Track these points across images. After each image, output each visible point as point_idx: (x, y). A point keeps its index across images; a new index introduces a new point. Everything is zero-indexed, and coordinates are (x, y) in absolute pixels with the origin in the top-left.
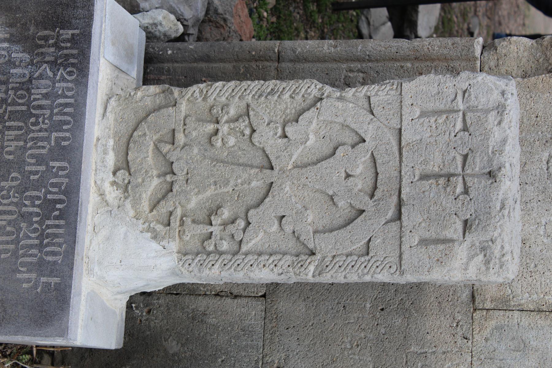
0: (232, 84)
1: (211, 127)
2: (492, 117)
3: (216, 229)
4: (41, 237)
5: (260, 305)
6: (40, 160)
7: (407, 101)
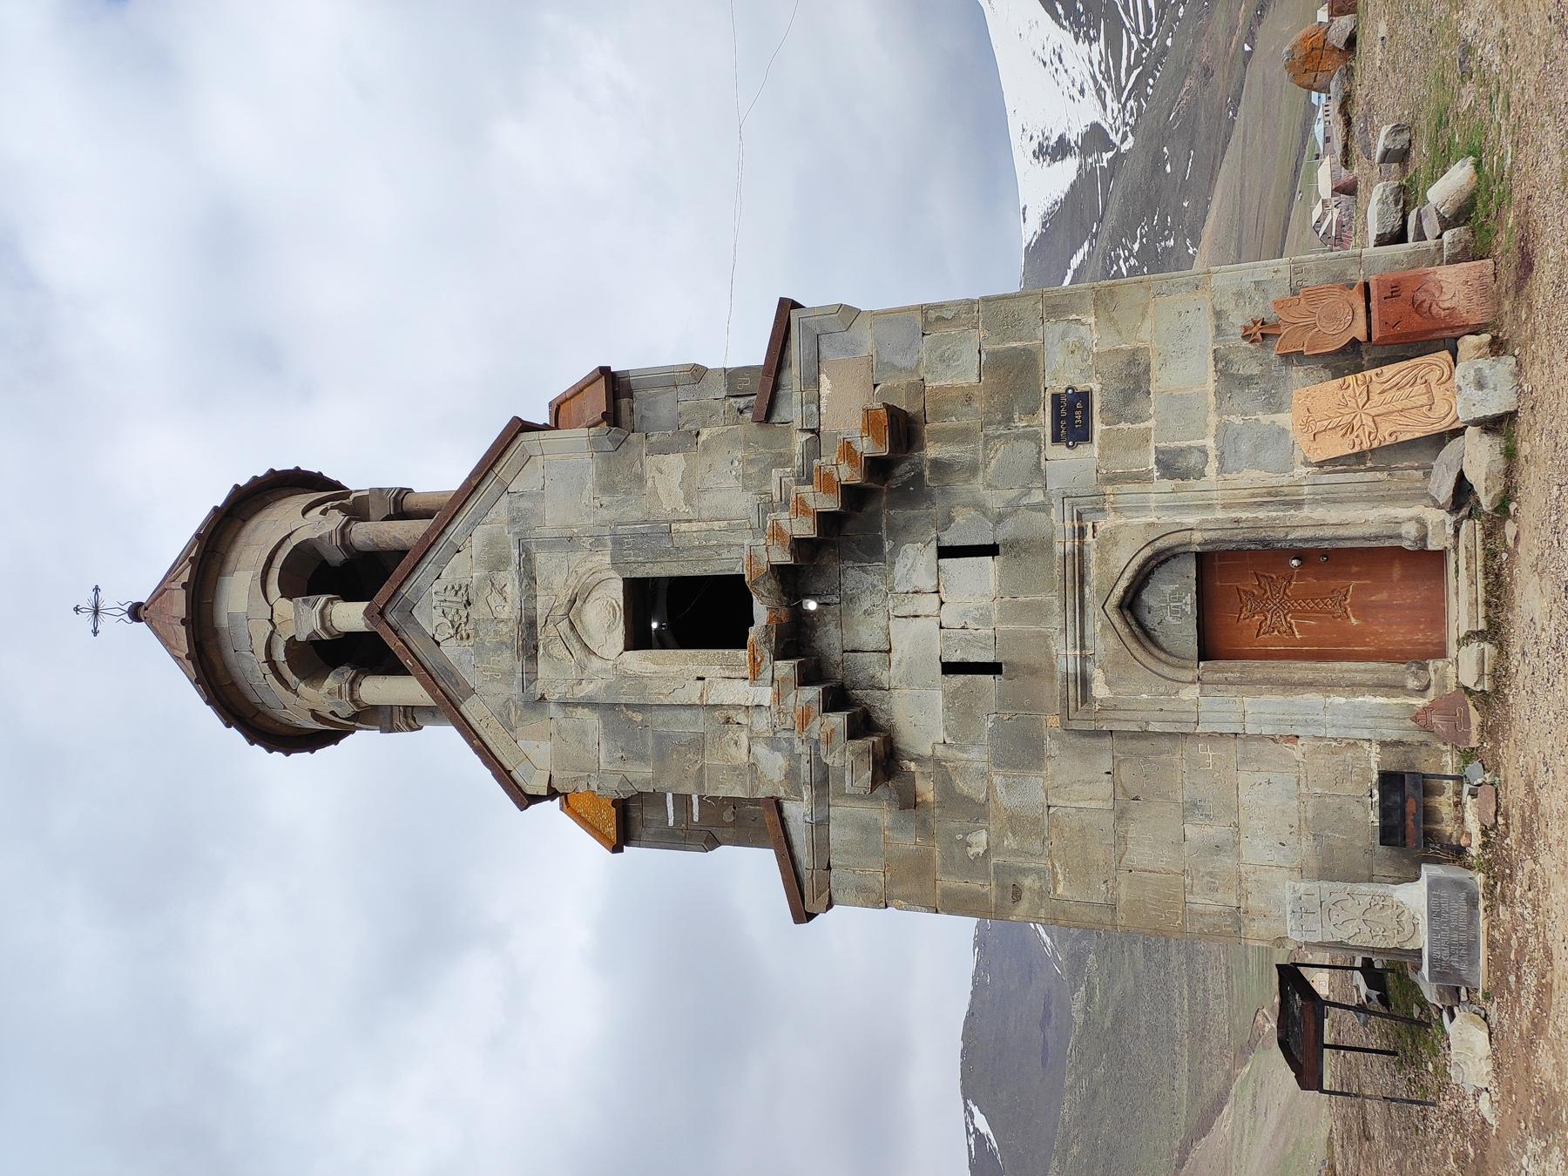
0: (1379, 946)
1: (1385, 934)
3: (1381, 903)
6: (1444, 930)
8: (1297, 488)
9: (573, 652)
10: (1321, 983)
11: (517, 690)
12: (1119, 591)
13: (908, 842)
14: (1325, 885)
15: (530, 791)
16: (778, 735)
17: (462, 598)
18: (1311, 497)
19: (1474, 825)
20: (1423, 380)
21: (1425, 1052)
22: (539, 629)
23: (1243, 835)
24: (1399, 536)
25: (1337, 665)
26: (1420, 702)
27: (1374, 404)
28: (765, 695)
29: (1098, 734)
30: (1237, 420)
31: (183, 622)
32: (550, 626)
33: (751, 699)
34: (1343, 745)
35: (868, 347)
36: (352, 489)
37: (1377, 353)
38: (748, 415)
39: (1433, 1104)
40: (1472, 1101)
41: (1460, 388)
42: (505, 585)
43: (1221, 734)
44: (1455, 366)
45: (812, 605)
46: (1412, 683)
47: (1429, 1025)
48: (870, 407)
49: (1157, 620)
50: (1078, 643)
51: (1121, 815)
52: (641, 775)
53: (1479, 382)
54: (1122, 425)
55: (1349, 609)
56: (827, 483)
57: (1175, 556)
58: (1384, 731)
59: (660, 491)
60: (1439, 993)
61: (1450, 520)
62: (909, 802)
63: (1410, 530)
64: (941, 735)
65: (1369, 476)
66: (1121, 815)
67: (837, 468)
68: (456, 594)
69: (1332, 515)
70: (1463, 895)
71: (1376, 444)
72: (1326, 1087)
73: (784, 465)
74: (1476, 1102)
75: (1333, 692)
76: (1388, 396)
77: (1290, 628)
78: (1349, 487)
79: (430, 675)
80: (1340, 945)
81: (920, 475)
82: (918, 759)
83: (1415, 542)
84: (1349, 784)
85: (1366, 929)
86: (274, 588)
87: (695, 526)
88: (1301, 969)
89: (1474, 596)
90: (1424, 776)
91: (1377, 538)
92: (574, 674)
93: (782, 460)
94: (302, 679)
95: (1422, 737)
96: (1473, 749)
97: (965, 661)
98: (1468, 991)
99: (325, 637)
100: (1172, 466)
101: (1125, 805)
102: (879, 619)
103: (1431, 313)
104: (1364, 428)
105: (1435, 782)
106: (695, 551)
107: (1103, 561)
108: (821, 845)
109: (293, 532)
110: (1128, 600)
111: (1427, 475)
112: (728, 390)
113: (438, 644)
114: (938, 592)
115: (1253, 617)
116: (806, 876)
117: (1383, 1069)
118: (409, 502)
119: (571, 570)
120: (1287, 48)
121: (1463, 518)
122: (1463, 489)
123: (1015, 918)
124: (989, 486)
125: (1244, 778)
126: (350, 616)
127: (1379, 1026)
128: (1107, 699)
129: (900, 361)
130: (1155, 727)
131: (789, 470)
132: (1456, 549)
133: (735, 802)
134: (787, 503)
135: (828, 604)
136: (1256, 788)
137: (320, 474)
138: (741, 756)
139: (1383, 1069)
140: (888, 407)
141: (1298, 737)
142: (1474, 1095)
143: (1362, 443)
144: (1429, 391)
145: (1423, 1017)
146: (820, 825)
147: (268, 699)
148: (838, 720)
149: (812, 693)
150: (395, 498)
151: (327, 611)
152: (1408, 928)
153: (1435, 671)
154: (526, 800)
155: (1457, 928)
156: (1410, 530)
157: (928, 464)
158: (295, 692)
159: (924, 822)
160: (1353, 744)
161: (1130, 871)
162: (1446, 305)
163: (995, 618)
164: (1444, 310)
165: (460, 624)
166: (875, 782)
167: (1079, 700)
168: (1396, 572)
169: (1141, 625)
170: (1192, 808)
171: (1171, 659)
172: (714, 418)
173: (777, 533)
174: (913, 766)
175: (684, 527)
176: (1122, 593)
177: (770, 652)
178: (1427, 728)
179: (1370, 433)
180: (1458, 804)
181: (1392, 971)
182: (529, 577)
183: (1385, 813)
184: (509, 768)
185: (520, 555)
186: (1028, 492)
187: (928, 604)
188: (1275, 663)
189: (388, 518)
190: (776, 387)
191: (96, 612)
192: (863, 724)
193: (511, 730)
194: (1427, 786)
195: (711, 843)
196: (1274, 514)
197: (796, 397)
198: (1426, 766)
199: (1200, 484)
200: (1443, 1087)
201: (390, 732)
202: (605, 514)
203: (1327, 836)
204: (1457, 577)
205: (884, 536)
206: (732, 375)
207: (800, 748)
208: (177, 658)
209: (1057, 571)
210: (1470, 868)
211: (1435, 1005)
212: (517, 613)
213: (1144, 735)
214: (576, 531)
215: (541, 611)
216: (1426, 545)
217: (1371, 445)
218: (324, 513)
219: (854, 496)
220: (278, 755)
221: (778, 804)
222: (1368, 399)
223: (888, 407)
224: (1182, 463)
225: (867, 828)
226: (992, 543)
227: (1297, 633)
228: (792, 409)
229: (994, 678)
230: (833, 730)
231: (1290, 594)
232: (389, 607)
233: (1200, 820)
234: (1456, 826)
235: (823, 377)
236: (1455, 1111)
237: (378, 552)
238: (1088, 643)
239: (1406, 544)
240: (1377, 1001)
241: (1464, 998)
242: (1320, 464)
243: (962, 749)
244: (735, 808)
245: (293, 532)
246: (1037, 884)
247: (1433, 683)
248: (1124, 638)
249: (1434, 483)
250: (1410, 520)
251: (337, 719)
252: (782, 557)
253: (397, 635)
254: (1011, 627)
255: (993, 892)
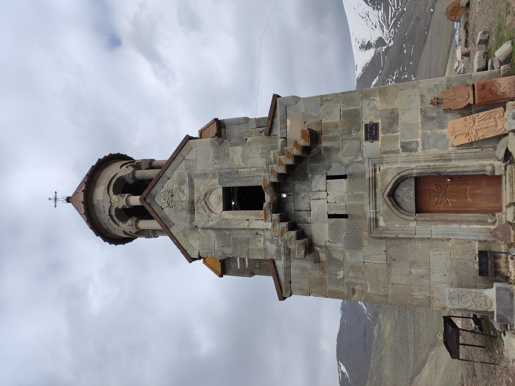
0: (479, 310)
2: (449, 304)
4: (500, 297)
5: (477, 285)
7: (458, 306)
8: (450, 155)
9: (206, 212)
10: (459, 323)
11: (188, 224)
12: (388, 190)
13: (317, 274)
14: (460, 289)
15: (192, 257)
16: (274, 238)
17: (170, 194)
18: (454, 157)
19: (512, 269)
20: (494, 117)
21: (495, 347)
22: (195, 204)
23: (431, 272)
24: (485, 171)
25: (464, 215)
26: (493, 227)
27: (476, 126)
28: (269, 225)
29: (381, 238)
30: (429, 132)
31: (83, 203)
32: (199, 203)
33: (264, 227)
34: (466, 242)
35: (303, 110)
36: (136, 160)
37: (477, 108)
38: (263, 133)
39: (498, 364)
40: (512, 363)
41: (507, 119)
42: (184, 190)
43: (424, 238)
44: (505, 112)
45: (284, 196)
46: (490, 221)
47: (497, 338)
48: (303, 129)
49: (401, 200)
50: (374, 207)
51: (389, 265)
52: (229, 252)
53: (514, 117)
54: (389, 134)
55: (468, 196)
56: (289, 155)
57: (407, 178)
58: (480, 237)
59: (234, 158)
60: (500, 327)
61: (503, 165)
62: (317, 261)
63: (489, 169)
64: (328, 239)
65: (475, 150)
66: (389, 265)
67: (293, 150)
68: (169, 192)
69: (462, 164)
70: (509, 293)
71: (477, 139)
72: (461, 358)
73: (275, 149)
74: (513, 364)
75: (462, 224)
76: (481, 123)
77: (448, 202)
78: (467, 154)
79: (160, 219)
80: (465, 310)
81: (320, 152)
82: (320, 247)
83: (491, 172)
84: (468, 255)
85: (474, 304)
86: (111, 192)
87: (246, 170)
88: (452, 318)
89: (512, 191)
90: (494, 252)
91: (477, 171)
92: (206, 218)
93: (275, 148)
94: (121, 221)
95: (494, 239)
96: (512, 243)
97: (336, 214)
98: (510, 326)
99: (127, 207)
100: (406, 147)
101: (390, 261)
102: (307, 200)
103: (496, 94)
104: (472, 134)
105: (498, 254)
106: (246, 178)
107: (383, 180)
108: (288, 274)
109: (117, 174)
110: (391, 193)
111: (495, 150)
112: (257, 125)
113: (163, 209)
114: (326, 191)
115: (435, 198)
116: (283, 285)
117: (481, 353)
118: (154, 163)
119: (205, 185)
120: (446, 7)
121: (508, 164)
122: (508, 154)
123: (353, 300)
124: (344, 155)
125: (432, 253)
126: (135, 200)
127: (479, 338)
128: (384, 226)
129: (314, 114)
130: (401, 236)
131: (277, 151)
132: (505, 175)
133: (260, 261)
134: (276, 162)
135: (290, 195)
136: (436, 256)
137: (126, 155)
138: (261, 245)
139: (481, 353)
140: (309, 129)
141: (450, 239)
142: (512, 361)
143: (472, 139)
144: (496, 121)
145: (494, 335)
146: (288, 268)
147: (110, 228)
148: (293, 233)
149: (284, 224)
150: (149, 162)
151: (128, 198)
152: (489, 304)
153: (498, 217)
154: (191, 260)
155: (506, 304)
156: (489, 169)
157: (323, 148)
158: (118, 225)
159: (322, 267)
160: (469, 242)
161: (392, 284)
162: (502, 91)
163: (346, 199)
164: (501, 93)
165: (170, 202)
166: (306, 254)
167: (375, 226)
168: (484, 183)
169: (396, 201)
170: (413, 263)
171: (406, 213)
172: (252, 135)
173: (273, 171)
174: (318, 249)
175: (242, 170)
176: (389, 191)
177: (271, 211)
178: (495, 236)
179: (475, 136)
180: (507, 262)
181: (484, 319)
182: (192, 187)
183: (480, 265)
184: (186, 249)
185: (189, 180)
186: (356, 156)
187: (323, 195)
188: (442, 214)
189: (147, 169)
190: (272, 124)
191: (56, 200)
192: (302, 235)
193: (186, 237)
194: (495, 256)
195: (252, 274)
196: (442, 163)
197: (279, 127)
198: (495, 249)
199: (416, 154)
200: (502, 358)
201: (148, 238)
202: (216, 166)
203: (460, 273)
204: (506, 184)
205: (308, 172)
206: (258, 120)
207: (281, 243)
208: (81, 214)
209: (367, 184)
210: (511, 284)
211: (499, 331)
212: (188, 199)
213: (397, 238)
214: (207, 172)
215: (196, 198)
216: (494, 174)
217: (475, 140)
218: (127, 167)
219: (298, 159)
220: (113, 245)
221: (274, 261)
222: (474, 124)
223: (309, 129)
224: (410, 147)
225: (303, 269)
226: (345, 174)
227: (450, 204)
228: (277, 131)
229: (346, 219)
230: (291, 237)
231: (447, 191)
232: (147, 197)
233: (416, 267)
234: (506, 269)
235: (288, 120)
236: (506, 367)
237: (144, 180)
238: (378, 208)
239: (488, 173)
240: (478, 329)
241: (509, 328)
242: (458, 146)
243: (335, 243)
244: (260, 263)
245: (117, 174)
246: (361, 288)
247: (497, 221)
248: (390, 206)
249: (497, 152)
250: (489, 165)
251: (132, 234)
252: (274, 179)
253: (150, 206)
254: (351, 202)
255: (346, 291)
